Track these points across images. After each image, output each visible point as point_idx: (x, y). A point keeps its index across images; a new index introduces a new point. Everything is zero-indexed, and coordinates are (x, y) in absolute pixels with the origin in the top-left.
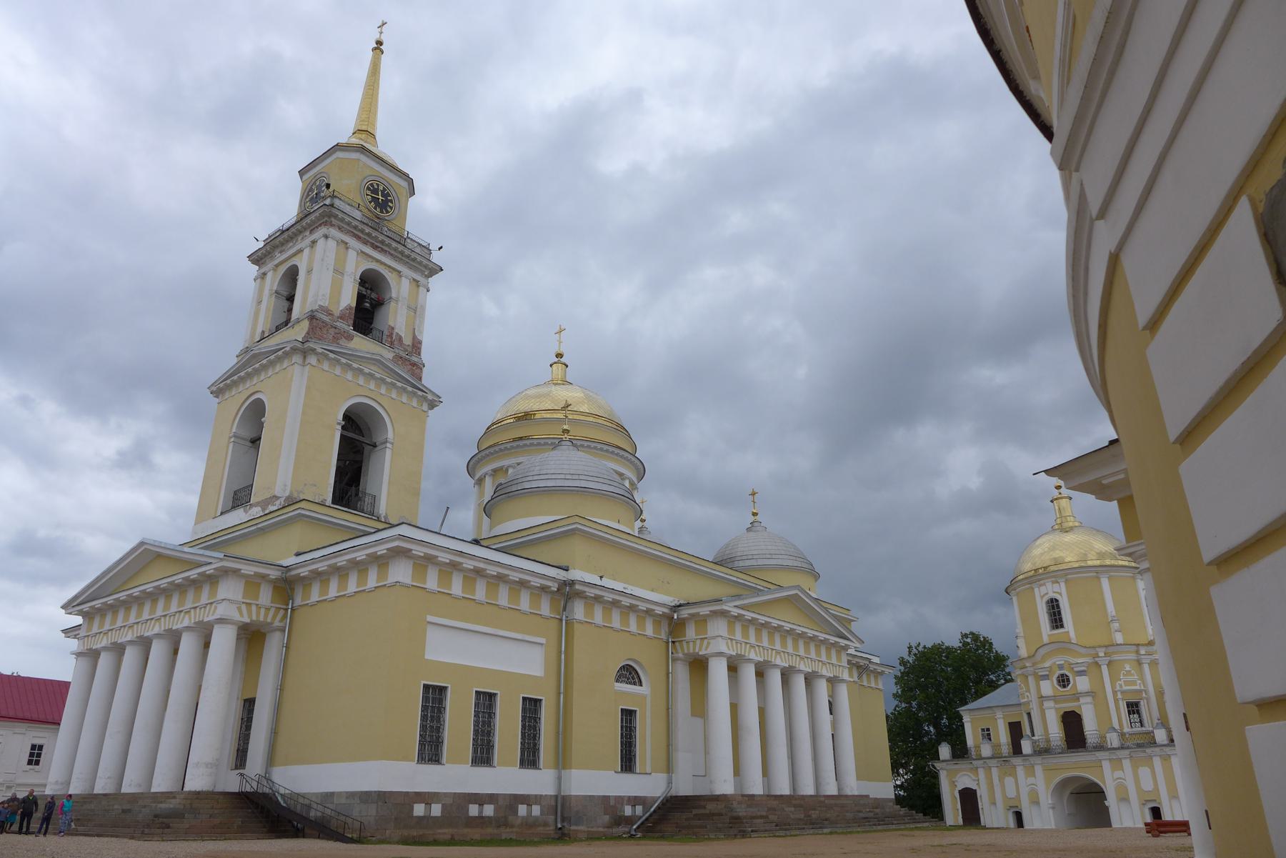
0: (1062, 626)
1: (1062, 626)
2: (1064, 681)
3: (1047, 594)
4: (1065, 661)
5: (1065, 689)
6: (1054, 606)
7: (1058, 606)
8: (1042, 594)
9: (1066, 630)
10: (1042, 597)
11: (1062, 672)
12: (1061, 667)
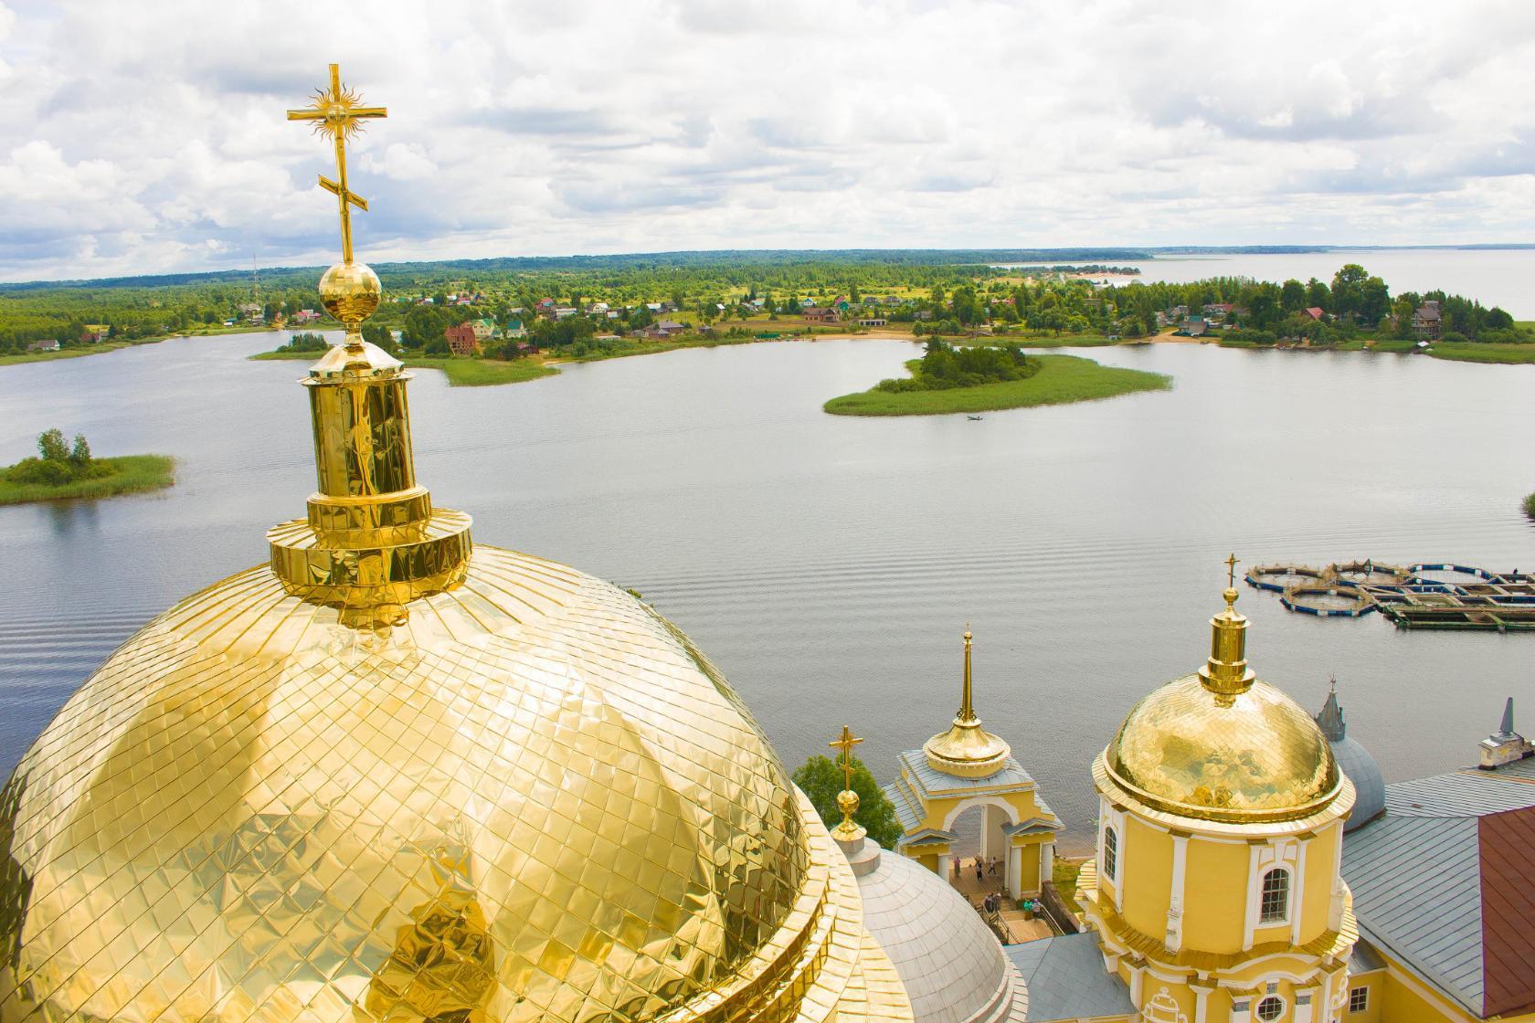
0: (1282, 916)
1: (1282, 916)
3: (1274, 861)
4: (1282, 979)
6: (1275, 886)
7: (1284, 885)
8: (1261, 863)
9: (1288, 923)
10: (1260, 867)
11: (1271, 996)
12: (1272, 988)
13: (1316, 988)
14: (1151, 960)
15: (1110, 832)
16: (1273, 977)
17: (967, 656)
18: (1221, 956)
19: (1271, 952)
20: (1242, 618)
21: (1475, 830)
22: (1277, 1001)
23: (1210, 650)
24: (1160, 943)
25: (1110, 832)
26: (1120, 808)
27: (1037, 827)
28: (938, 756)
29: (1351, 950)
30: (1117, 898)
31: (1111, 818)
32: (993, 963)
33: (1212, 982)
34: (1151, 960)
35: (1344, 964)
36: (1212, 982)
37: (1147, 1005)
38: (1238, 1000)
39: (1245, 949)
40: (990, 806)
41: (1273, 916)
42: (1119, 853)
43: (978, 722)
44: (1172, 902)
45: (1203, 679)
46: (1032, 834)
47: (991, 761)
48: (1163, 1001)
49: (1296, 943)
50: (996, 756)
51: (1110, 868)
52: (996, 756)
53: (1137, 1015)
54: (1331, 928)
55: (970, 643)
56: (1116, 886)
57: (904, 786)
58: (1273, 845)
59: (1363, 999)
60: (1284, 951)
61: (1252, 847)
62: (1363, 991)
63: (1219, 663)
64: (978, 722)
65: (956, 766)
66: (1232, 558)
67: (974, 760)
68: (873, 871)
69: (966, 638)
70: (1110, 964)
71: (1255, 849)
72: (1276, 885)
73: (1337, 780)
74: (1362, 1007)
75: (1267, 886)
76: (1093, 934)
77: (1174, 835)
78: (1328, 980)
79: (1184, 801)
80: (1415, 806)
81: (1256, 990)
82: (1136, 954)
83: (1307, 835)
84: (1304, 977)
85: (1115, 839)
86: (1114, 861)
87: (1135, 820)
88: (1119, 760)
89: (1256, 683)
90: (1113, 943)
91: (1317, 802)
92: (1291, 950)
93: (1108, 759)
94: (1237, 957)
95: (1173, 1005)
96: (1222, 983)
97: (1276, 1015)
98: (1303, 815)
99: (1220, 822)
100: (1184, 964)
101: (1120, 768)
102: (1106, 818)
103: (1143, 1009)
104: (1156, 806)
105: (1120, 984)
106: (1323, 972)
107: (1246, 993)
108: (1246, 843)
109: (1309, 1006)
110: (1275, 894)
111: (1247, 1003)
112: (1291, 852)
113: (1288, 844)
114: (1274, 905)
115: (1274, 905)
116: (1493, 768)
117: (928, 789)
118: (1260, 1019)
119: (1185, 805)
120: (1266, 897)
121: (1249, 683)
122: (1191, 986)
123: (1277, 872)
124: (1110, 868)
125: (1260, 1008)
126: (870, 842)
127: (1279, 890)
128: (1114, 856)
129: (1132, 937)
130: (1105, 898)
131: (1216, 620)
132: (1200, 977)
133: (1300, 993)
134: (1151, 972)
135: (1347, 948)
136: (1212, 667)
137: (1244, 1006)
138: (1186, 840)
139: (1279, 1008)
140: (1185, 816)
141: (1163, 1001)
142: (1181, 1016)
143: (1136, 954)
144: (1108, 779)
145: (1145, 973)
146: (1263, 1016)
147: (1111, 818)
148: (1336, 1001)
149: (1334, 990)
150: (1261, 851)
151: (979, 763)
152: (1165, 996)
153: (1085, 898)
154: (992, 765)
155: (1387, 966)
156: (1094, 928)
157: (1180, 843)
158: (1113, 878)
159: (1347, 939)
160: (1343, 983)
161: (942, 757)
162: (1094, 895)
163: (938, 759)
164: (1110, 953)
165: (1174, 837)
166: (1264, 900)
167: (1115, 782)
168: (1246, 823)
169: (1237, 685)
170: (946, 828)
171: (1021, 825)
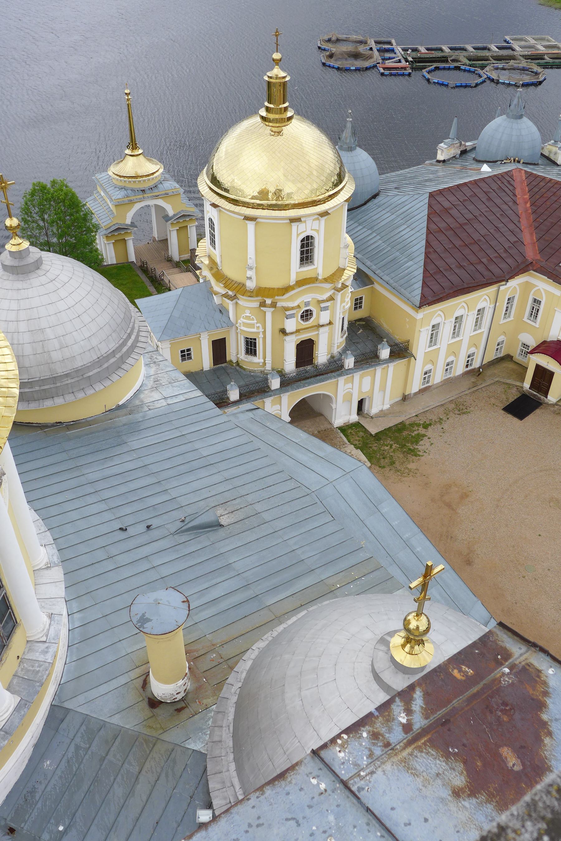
2: (307, 315)
3: (306, 231)
4: (312, 298)
5: (307, 323)
7: (312, 244)
9: (315, 267)
12: (307, 304)
13: (332, 302)
14: (239, 296)
15: (211, 220)
16: (307, 298)
17: (128, 106)
18: (278, 289)
19: (309, 283)
20: (283, 74)
21: (427, 201)
22: (311, 311)
23: (266, 97)
24: (244, 285)
25: (211, 220)
26: (214, 205)
27: (184, 216)
28: (118, 175)
29: (352, 278)
30: (218, 260)
31: (210, 212)
32: (122, 317)
33: (274, 305)
34: (239, 296)
35: (348, 286)
36: (274, 305)
37: (239, 321)
38: (288, 313)
39: (291, 284)
40: (157, 206)
41: (307, 263)
42: (216, 233)
43: (140, 151)
44: (248, 261)
45: (263, 118)
46: (181, 221)
47: (151, 177)
48: (247, 318)
49: (320, 278)
50: (155, 173)
51: (213, 242)
52: (155, 173)
53: (234, 327)
54: (341, 267)
55: (130, 97)
56: (216, 254)
57: (99, 197)
58: (305, 221)
59: (361, 303)
60: (313, 283)
61: (292, 224)
62: (361, 298)
63: (271, 106)
64: (140, 151)
65: (130, 182)
66: (277, 32)
67: (142, 177)
68: (38, 268)
69: (126, 94)
70: (217, 300)
71: (294, 225)
72: (308, 245)
73: (344, 178)
74: (360, 307)
75: (302, 246)
76: (207, 282)
77: (247, 220)
78: (339, 296)
79: (252, 198)
80: (396, 188)
81: (299, 307)
82: (230, 293)
83: (325, 214)
84: (325, 296)
85: (214, 225)
86: (214, 238)
87: (226, 213)
88: (213, 175)
89: (294, 121)
90: (218, 288)
91: (331, 193)
92: (317, 282)
93: (207, 174)
94: (286, 290)
95: (253, 319)
96: (279, 304)
97: (310, 318)
98: (324, 201)
99: (273, 210)
100: (257, 296)
101: (214, 180)
102: (208, 212)
103: (237, 324)
104: (235, 202)
105: (222, 310)
106: (337, 292)
107: (293, 308)
108: (288, 221)
109: (328, 312)
110: (307, 250)
111: (294, 314)
112: (316, 225)
113: (314, 220)
114: (307, 257)
115: (307, 257)
116: (444, 161)
117: (113, 198)
118: (302, 322)
119: (253, 201)
120: (302, 253)
121: (290, 118)
122: (262, 308)
123: (308, 237)
124: (213, 242)
125: (301, 316)
126: (33, 249)
127: (309, 248)
128: (214, 235)
129: (226, 282)
130: (213, 262)
131: (269, 77)
132: (267, 302)
133: (323, 305)
134: (239, 302)
135: (349, 277)
136: (268, 110)
137: (292, 316)
138: (254, 223)
139: (311, 314)
140: (253, 208)
141: (247, 318)
142: (258, 325)
143: (230, 293)
144: (207, 187)
145: (237, 303)
146: (303, 320)
147: (210, 212)
148: (344, 306)
149: (343, 301)
150: (298, 226)
151: (144, 178)
152: (248, 315)
153: (202, 262)
154: (153, 179)
155: (373, 283)
156: (207, 279)
157: (251, 226)
158: (215, 249)
159: (350, 273)
160: (348, 296)
161: (120, 176)
162: (206, 262)
163: (117, 177)
164: (216, 293)
165: (247, 222)
166: (301, 255)
167: (211, 189)
168: (289, 209)
169: (282, 121)
170: (128, 221)
171: (174, 215)
